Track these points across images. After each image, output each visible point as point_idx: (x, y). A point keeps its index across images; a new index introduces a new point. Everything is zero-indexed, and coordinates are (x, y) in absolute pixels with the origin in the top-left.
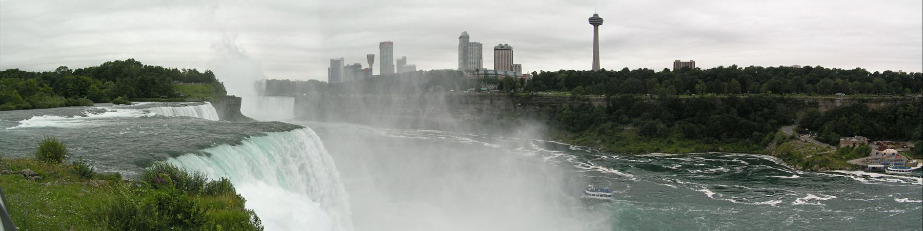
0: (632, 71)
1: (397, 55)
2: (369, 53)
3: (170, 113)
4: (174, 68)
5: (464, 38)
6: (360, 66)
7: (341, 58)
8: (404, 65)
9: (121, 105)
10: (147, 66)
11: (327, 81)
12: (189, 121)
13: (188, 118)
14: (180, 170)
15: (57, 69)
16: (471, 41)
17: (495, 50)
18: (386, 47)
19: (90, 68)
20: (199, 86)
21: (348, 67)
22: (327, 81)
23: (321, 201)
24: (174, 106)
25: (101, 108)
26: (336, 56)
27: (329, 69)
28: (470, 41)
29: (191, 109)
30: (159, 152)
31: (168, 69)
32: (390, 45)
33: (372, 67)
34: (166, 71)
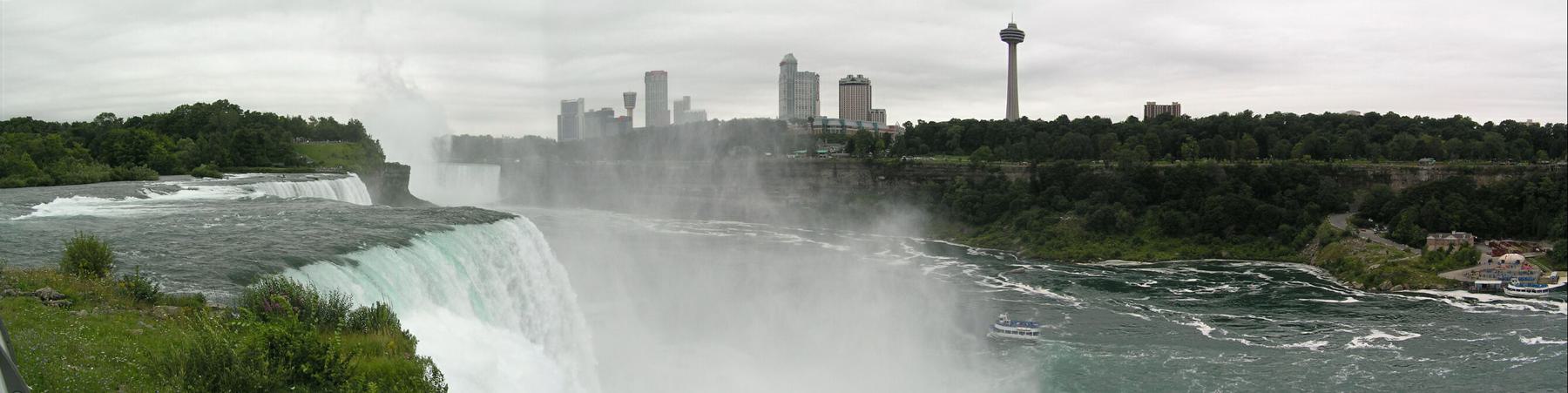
0: (1073, 121)
1: (674, 93)
2: (627, 91)
3: (289, 193)
4: (296, 115)
5: (789, 64)
6: (611, 112)
7: (580, 99)
8: (686, 111)
9: (205, 179)
10: (250, 112)
11: (555, 137)
12: (320, 206)
13: (319, 200)
14: (305, 289)
15: (97, 117)
16: (800, 69)
17: (840, 85)
18: (656, 80)
19: (153, 116)
20: (338, 146)
21: (591, 114)
22: (555, 137)
23: (546, 342)
24: (295, 181)
25: (171, 183)
26: (571, 96)
27: (559, 117)
28: (798, 70)
29: (325, 186)
30: (270, 259)
31: (286, 117)
32: (663, 76)
33: (631, 114)
34: (283, 120)
